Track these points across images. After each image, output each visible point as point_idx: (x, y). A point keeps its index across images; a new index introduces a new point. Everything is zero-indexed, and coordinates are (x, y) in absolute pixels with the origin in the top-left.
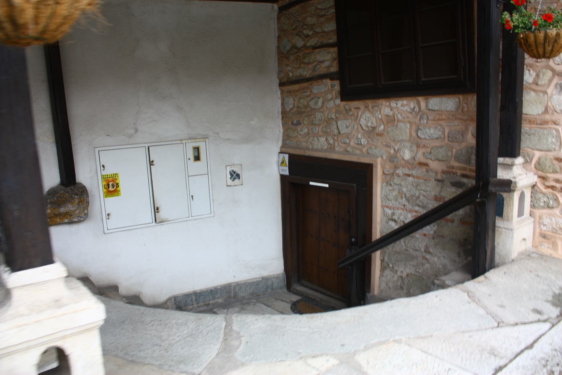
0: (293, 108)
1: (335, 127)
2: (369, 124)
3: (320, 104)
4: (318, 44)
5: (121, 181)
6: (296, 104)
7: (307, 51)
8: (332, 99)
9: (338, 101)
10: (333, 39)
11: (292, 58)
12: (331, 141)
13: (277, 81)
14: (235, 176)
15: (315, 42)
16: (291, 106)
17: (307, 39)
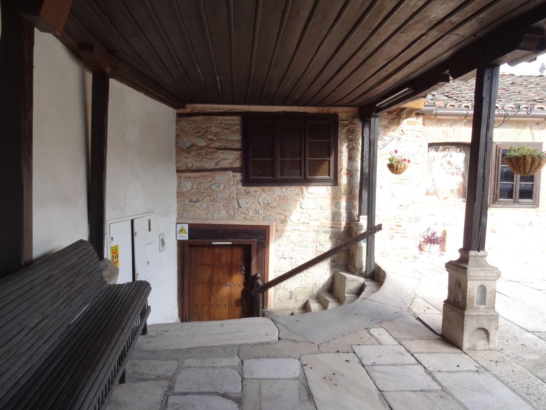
0: (192, 189)
1: (236, 203)
2: (266, 201)
3: (222, 187)
4: (222, 147)
5: (120, 253)
6: (195, 187)
7: (211, 150)
8: (234, 184)
9: (240, 186)
10: (238, 145)
11: (193, 153)
12: (232, 213)
13: (175, 169)
15: (219, 145)
16: (189, 188)
17: (210, 142)
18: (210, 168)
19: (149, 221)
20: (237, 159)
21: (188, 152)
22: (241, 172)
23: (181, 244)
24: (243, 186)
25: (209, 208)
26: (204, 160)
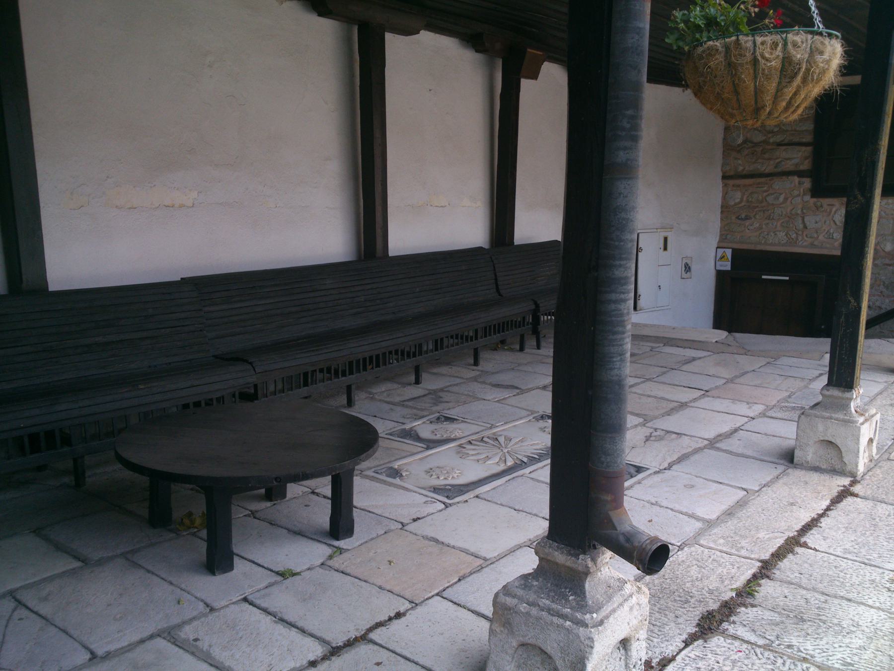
1: (800, 221)
4: (786, 141)
7: (769, 147)
8: (798, 195)
9: (807, 198)
10: (808, 138)
12: (794, 236)
13: (721, 174)
14: (687, 268)
16: (738, 201)
18: (767, 171)
19: (666, 239)
20: (806, 158)
21: (739, 151)
22: (811, 177)
23: (720, 274)
24: (812, 196)
25: (761, 228)
26: (760, 161)
